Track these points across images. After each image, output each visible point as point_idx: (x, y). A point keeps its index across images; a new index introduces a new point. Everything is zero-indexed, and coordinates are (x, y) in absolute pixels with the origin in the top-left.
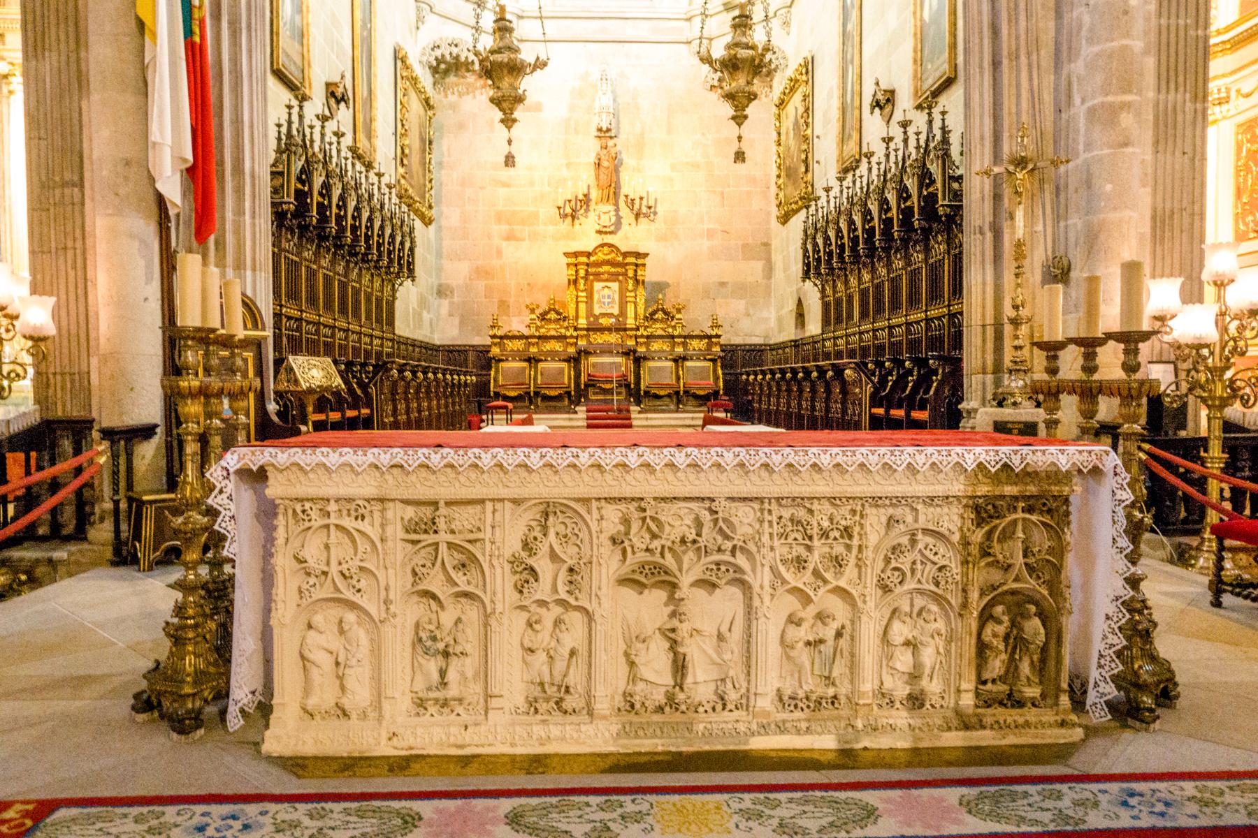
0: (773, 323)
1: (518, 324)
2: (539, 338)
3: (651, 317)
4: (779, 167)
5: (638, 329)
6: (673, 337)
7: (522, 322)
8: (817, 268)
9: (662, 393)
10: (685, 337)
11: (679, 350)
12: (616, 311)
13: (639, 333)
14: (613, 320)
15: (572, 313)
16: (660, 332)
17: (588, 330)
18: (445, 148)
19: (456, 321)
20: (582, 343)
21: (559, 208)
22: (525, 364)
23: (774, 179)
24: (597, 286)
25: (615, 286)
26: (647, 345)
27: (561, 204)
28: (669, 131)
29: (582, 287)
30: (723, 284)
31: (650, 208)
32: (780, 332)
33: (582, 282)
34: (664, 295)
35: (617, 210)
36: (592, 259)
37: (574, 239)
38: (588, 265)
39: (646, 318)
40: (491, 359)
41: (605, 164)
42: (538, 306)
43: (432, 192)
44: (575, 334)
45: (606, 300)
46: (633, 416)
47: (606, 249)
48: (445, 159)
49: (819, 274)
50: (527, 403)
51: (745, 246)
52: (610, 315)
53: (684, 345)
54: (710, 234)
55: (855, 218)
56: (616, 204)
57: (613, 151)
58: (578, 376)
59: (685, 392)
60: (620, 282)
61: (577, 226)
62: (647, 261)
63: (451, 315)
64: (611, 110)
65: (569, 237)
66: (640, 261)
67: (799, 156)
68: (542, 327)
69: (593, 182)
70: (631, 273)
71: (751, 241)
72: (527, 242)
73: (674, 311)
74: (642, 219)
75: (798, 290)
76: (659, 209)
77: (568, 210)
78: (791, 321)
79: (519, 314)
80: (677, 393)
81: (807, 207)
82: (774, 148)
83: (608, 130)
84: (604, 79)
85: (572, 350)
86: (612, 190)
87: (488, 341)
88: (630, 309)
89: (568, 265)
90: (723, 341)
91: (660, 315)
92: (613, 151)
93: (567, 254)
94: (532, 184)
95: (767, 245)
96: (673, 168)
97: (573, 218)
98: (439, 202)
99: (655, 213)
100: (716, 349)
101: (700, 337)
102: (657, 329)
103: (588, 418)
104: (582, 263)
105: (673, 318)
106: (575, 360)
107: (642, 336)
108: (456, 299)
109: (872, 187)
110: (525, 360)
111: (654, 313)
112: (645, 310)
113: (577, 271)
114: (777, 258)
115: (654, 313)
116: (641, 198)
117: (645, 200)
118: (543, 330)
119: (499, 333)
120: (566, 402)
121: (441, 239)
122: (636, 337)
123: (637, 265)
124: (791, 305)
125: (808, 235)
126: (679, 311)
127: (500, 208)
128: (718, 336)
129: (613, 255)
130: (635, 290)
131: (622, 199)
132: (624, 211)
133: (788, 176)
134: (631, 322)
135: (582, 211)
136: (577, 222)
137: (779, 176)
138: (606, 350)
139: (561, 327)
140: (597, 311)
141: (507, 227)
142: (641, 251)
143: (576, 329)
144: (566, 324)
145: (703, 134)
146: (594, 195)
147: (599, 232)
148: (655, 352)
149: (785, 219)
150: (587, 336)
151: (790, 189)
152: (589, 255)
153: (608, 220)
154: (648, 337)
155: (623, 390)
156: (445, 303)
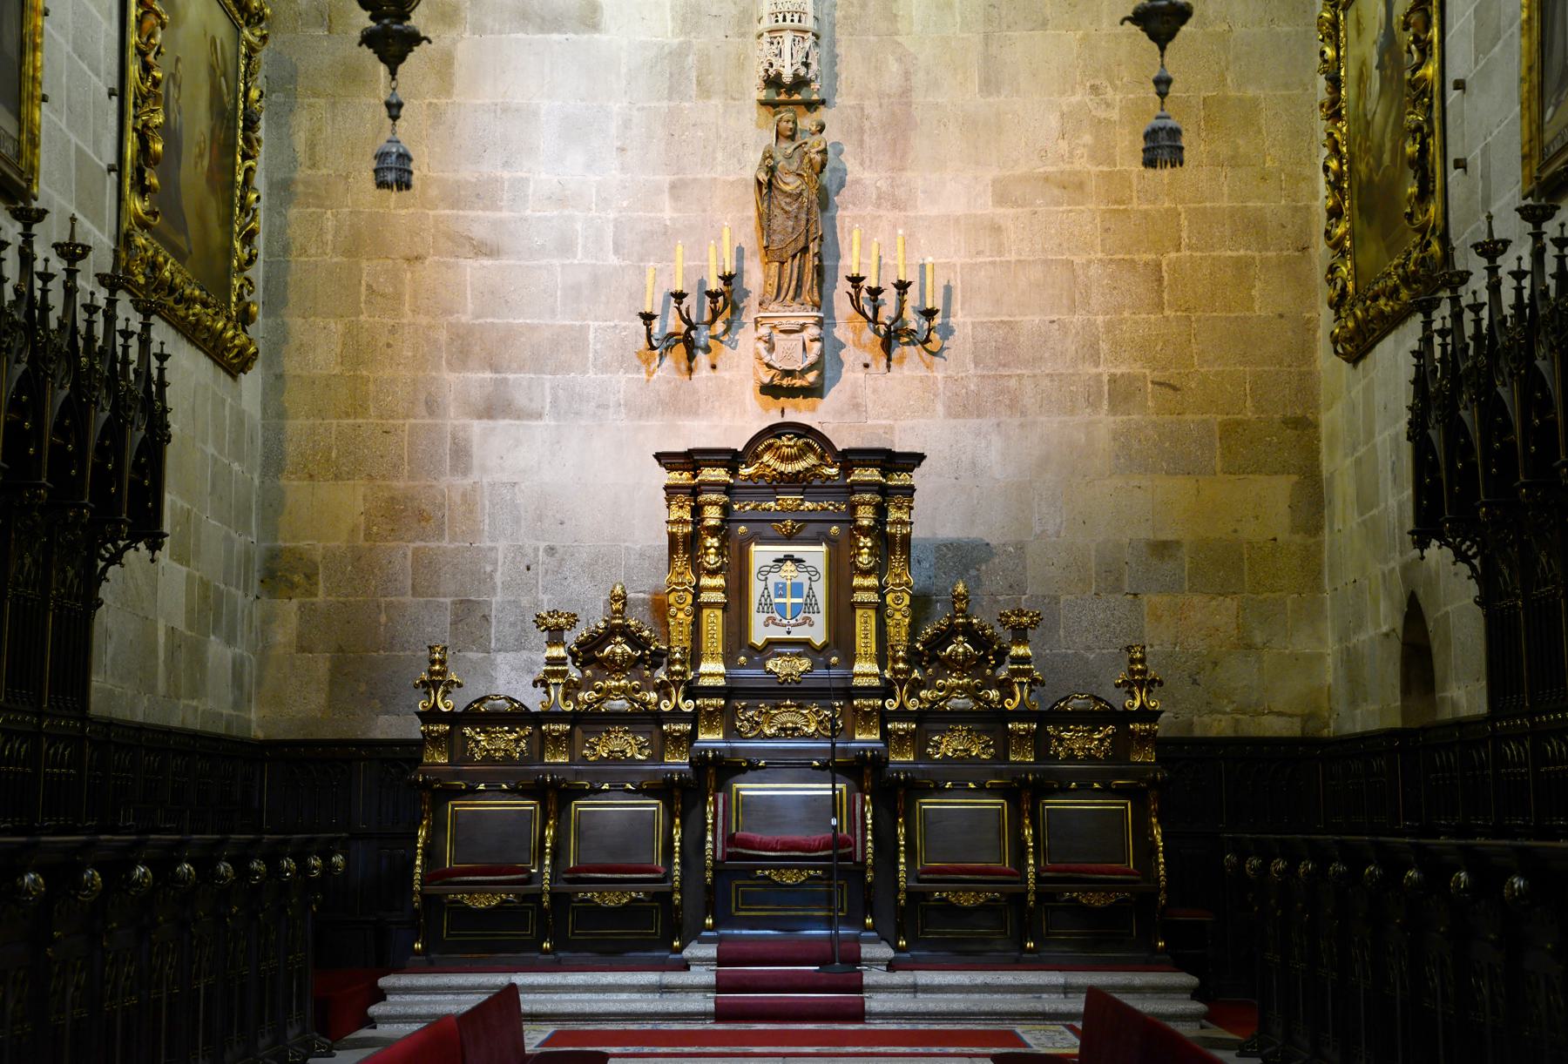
0: (1330, 674)
2: (575, 718)
3: (929, 655)
4: (1335, 185)
9: (967, 900)
10: (1042, 717)
12: (818, 633)
13: (892, 705)
14: (805, 664)
15: (680, 639)
16: (960, 702)
17: (728, 692)
20: (711, 738)
21: (648, 318)
22: (529, 805)
23: (1321, 221)
24: (761, 555)
25: (816, 555)
26: (918, 741)
28: (990, 84)
29: (712, 559)
30: (1162, 549)
31: (929, 314)
32: (1353, 703)
37: (693, 411)
38: (728, 489)
39: (913, 658)
41: (790, 184)
42: (573, 620)
44: (687, 706)
47: (787, 443)
48: (302, 173)
51: (1230, 430)
53: (1040, 742)
56: (822, 303)
58: (694, 846)
60: (831, 542)
62: (917, 478)
64: (809, 23)
65: (677, 405)
66: (899, 479)
67: (1397, 150)
69: (749, 236)
70: (865, 517)
71: (1250, 415)
72: (548, 421)
73: (1006, 635)
75: (1406, 569)
76: (959, 319)
78: (1386, 673)
79: (520, 646)
80: (1019, 899)
82: (1321, 125)
83: (800, 83)
85: (678, 761)
86: (811, 262)
87: (416, 730)
88: (864, 627)
89: (671, 491)
91: (959, 647)
93: (666, 460)
94: (565, 246)
95: (1304, 427)
96: (1001, 198)
97: (691, 348)
98: (275, 302)
99: (947, 331)
100: (1144, 756)
101: (1089, 719)
103: (720, 987)
104: (714, 486)
105: (1002, 655)
107: (902, 714)
108: (321, 598)
110: (526, 793)
111: (944, 638)
113: (697, 511)
114: (1337, 465)
115: (944, 638)
116: (902, 287)
117: (912, 292)
121: (281, 414)
122: (884, 716)
123: (883, 490)
124: (1385, 618)
126: (1020, 635)
127: (464, 319)
129: (811, 460)
130: (879, 570)
133: (1366, 210)
136: (702, 359)
137: (1335, 213)
139: (648, 685)
140: (759, 633)
141: (488, 375)
143: (692, 692)
144: (661, 675)
145: (1095, 89)
146: (755, 277)
147: (770, 390)
150: (726, 719)
151: (1372, 250)
152: (731, 459)
154: (919, 717)
156: (289, 608)
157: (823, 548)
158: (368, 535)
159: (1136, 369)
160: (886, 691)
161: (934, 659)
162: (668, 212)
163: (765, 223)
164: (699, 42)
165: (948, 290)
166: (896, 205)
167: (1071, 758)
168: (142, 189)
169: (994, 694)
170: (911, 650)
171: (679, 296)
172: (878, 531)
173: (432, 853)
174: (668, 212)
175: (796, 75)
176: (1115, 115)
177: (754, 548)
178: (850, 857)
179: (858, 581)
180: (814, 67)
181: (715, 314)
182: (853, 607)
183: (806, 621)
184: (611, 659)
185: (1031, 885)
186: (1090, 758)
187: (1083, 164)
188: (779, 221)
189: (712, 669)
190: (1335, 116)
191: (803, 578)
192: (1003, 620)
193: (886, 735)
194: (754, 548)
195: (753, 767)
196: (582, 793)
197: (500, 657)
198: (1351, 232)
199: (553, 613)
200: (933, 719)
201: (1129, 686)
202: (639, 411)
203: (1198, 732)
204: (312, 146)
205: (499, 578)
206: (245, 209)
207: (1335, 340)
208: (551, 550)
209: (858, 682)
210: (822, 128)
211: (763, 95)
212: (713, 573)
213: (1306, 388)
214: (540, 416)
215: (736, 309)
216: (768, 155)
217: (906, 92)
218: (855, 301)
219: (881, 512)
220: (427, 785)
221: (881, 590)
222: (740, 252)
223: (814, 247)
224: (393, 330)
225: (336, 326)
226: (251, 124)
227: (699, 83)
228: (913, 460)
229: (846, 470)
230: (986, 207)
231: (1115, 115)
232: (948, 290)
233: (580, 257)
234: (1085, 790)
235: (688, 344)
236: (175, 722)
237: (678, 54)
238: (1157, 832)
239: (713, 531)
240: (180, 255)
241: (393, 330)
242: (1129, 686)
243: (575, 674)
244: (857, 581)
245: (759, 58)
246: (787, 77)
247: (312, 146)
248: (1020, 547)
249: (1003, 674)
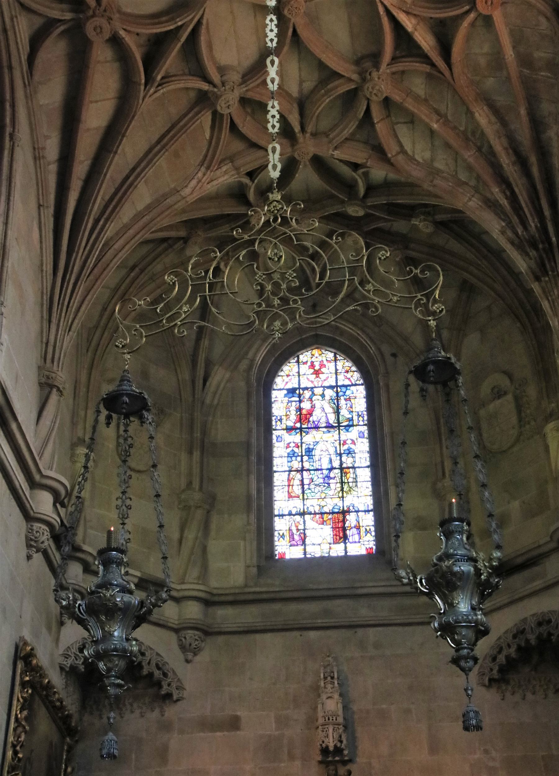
83: (338, 751)
145: (486, 752)
175: (335, 746)
180: (345, 742)
211: (320, 758)
227: (289, 753)
246: (331, 748)
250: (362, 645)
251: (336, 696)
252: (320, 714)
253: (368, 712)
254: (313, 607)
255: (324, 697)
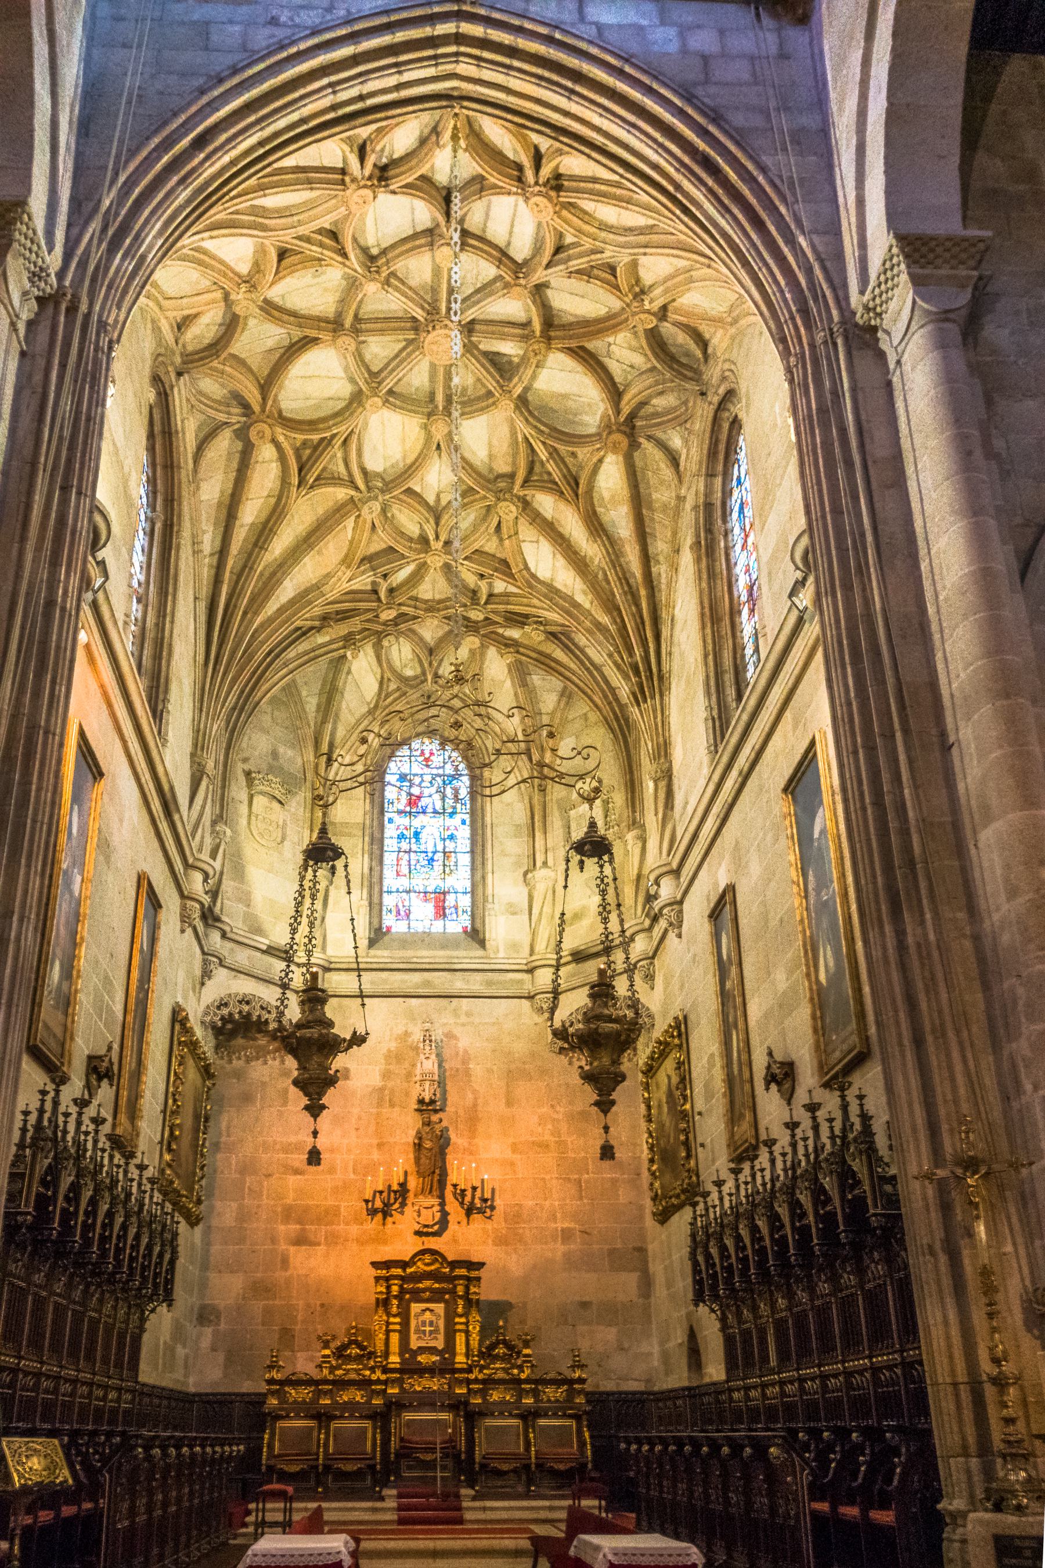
1: (304, 1364)
2: (334, 1382)
3: (488, 1354)
4: (651, 1149)
5: (469, 1370)
6: (518, 1381)
7: (311, 1359)
8: (714, 1287)
9: (505, 1467)
10: (536, 1382)
11: (528, 1401)
12: (440, 1344)
13: (472, 1376)
15: (380, 1346)
16: (501, 1375)
18: (224, 1125)
19: (221, 1357)
20: (393, 1391)
21: (367, 1201)
22: (312, 1423)
23: (646, 1164)
24: (416, 1307)
25: (439, 1308)
26: (483, 1393)
27: (368, 1195)
28: (509, 1103)
29: (394, 1310)
30: (585, 1305)
31: (485, 1201)
32: (667, 1374)
33: (395, 1302)
34: (506, 1321)
35: (442, 1204)
36: (409, 1270)
38: (401, 1278)
39: (481, 1355)
40: (265, 1415)
41: (428, 1144)
42: (334, 1338)
43: (203, 1182)
44: (383, 1377)
45: (428, 1329)
46: (465, 1504)
47: (428, 1258)
48: (223, 1139)
49: (715, 1297)
50: (313, 1483)
51: (612, 1252)
52: (432, 1350)
53: (535, 1393)
54: (567, 1235)
55: (760, 1223)
56: (442, 1196)
57: (438, 1128)
58: (386, 1442)
59: (538, 1465)
60: (446, 1302)
61: (389, 1226)
62: (483, 1273)
63: (214, 1349)
64: (436, 1078)
65: (379, 1239)
68: (338, 1367)
69: (411, 1168)
70: (460, 1290)
71: (619, 1246)
74: (475, 1216)
76: (498, 1202)
77: (378, 1204)
80: (527, 1467)
81: (694, 1205)
82: (643, 1125)
83: (432, 1102)
84: (427, 1038)
85: (377, 1401)
86: (436, 1178)
87: (264, 1388)
88: (460, 1339)
89: (377, 1279)
90: (588, 1387)
91: (501, 1350)
92: (438, 1128)
93: (375, 1265)
95: (641, 1250)
98: (210, 1195)
99: (492, 1208)
100: (580, 1400)
102: (497, 1369)
104: (396, 1277)
105: (519, 1353)
106: (382, 1417)
107: (476, 1381)
109: (778, 1185)
110: (312, 1417)
111: (493, 1346)
112: (481, 1342)
113: (388, 1288)
114: (657, 1269)
115: (493, 1346)
116: (474, 1189)
117: (479, 1191)
118: (339, 1372)
119: (277, 1375)
120: (369, 1481)
122: (468, 1382)
123: (468, 1279)
125: (698, 1243)
126: (527, 1344)
127: (289, 1201)
128: (581, 1381)
129: (437, 1265)
130: (465, 1314)
131: (449, 1190)
132: (453, 1206)
133: (663, 1159)
134: (460, 1359)
135: (397, 1206)
136: (389, 1219)
137: (652, 1161)
138: (427, 1401)
139: (366, 1368)
140: (414, 1343)
141: (298, 1227)
142: (475, 1259)
143: (385, 1370)
144: (372, 1363)
145: (552, 1106)
146: (413, 1183)
147: (418, 1233)
148: (495, 1403)
149: (663, 1217)
150: (400, 1382)
151: (668, 1177)
152: (404, 1265)
153: (430, 1216)
154: (484, 1382)
155: (450, 1463)
157: (442, 1305)
158: (244, 1298)
159: (572, 1225)
160: (469, 1370)
161: (490, 1355)
162: (376, 1156)
163: (417, 1160)
164: (390, 1084)
165: (493, 1190)
166: (471, 1153)
167: (549, 1401)
168: (170, 1150)
169: (515, 1371)
170: (480, 1351)
171: (381, 1192)
172: (466, 1297)
173: (271, 1447)
174: (376, 1156)
176: (561, 1117)
177: (413, 1305)
178: (454, 1447)
179: (457, 1320)
181: (396, 1200)
182: (456, 1331)
183: (436, 1338)
184: (349, 1356)
185: (533, 1460)
186: (557, 1401)
187: (547, 1137)
188: (423, 1160)
189: (394, 1359)
190: (650, 1121)
191: (434, 1318)
192: (519, 1337)
193: (469, 1390)
194: (413, 1305)
195: (411, 1405)
196: (335, 1418)
197: (299, 1354)
198: (659, 1169)
199: (325, 1334)
200: (489, 1382)
201: (573, 1367)
202: (361, 1242)
203: (602, 1389)
204: (228, 1128)
205: (299, 1318)
206: (202, 1155)
207: (654, 1214)
208: (322, 1305)
209: (457, 1366)
210: (441, 1121)
212: (395, 1316)
213: (642, 1234)
214: (319, 1244)
215: (405, 1199)
216: (418, 1132)
217: (475, 1105)
218: (455, 1194)
219: (467, 1288)
220: (270, 1413)
221: (467, 1324)
222: (406, 1173)
223: (437, 1171)
224: (259, 1206)
225: (234, 1205)
226: (207, 1120)
228: (481, 1265)
229: (452, 1270)
230: (509, 1154)
231: (561, 1117)
232: (493, 1190)
233: (339, 1175)
234: (555, 1415)
235: (386, 1213)
236: (164, 1384)
237: (382, 1090)
238: (587, 1434)
239: (396, 1297)
240: (178, 1176)
241: (259, 1206)
242: (573, 1367)
243: (334, 1363)
244: (457, 1320)
245: (416, 1092)
246: (427, 1100)
247: (228, 1128)
248: (525, 1304)
249: (519, 1362)
250: (456, 1013)
251: (433, 1057)
252: (418, 1071)
253: (457, 1070)
254: (417, 977)
255: (422, 1057)
